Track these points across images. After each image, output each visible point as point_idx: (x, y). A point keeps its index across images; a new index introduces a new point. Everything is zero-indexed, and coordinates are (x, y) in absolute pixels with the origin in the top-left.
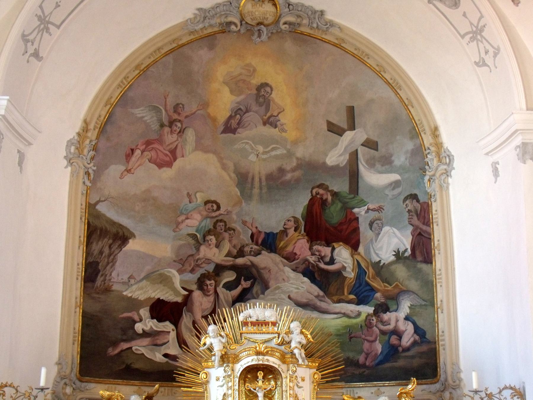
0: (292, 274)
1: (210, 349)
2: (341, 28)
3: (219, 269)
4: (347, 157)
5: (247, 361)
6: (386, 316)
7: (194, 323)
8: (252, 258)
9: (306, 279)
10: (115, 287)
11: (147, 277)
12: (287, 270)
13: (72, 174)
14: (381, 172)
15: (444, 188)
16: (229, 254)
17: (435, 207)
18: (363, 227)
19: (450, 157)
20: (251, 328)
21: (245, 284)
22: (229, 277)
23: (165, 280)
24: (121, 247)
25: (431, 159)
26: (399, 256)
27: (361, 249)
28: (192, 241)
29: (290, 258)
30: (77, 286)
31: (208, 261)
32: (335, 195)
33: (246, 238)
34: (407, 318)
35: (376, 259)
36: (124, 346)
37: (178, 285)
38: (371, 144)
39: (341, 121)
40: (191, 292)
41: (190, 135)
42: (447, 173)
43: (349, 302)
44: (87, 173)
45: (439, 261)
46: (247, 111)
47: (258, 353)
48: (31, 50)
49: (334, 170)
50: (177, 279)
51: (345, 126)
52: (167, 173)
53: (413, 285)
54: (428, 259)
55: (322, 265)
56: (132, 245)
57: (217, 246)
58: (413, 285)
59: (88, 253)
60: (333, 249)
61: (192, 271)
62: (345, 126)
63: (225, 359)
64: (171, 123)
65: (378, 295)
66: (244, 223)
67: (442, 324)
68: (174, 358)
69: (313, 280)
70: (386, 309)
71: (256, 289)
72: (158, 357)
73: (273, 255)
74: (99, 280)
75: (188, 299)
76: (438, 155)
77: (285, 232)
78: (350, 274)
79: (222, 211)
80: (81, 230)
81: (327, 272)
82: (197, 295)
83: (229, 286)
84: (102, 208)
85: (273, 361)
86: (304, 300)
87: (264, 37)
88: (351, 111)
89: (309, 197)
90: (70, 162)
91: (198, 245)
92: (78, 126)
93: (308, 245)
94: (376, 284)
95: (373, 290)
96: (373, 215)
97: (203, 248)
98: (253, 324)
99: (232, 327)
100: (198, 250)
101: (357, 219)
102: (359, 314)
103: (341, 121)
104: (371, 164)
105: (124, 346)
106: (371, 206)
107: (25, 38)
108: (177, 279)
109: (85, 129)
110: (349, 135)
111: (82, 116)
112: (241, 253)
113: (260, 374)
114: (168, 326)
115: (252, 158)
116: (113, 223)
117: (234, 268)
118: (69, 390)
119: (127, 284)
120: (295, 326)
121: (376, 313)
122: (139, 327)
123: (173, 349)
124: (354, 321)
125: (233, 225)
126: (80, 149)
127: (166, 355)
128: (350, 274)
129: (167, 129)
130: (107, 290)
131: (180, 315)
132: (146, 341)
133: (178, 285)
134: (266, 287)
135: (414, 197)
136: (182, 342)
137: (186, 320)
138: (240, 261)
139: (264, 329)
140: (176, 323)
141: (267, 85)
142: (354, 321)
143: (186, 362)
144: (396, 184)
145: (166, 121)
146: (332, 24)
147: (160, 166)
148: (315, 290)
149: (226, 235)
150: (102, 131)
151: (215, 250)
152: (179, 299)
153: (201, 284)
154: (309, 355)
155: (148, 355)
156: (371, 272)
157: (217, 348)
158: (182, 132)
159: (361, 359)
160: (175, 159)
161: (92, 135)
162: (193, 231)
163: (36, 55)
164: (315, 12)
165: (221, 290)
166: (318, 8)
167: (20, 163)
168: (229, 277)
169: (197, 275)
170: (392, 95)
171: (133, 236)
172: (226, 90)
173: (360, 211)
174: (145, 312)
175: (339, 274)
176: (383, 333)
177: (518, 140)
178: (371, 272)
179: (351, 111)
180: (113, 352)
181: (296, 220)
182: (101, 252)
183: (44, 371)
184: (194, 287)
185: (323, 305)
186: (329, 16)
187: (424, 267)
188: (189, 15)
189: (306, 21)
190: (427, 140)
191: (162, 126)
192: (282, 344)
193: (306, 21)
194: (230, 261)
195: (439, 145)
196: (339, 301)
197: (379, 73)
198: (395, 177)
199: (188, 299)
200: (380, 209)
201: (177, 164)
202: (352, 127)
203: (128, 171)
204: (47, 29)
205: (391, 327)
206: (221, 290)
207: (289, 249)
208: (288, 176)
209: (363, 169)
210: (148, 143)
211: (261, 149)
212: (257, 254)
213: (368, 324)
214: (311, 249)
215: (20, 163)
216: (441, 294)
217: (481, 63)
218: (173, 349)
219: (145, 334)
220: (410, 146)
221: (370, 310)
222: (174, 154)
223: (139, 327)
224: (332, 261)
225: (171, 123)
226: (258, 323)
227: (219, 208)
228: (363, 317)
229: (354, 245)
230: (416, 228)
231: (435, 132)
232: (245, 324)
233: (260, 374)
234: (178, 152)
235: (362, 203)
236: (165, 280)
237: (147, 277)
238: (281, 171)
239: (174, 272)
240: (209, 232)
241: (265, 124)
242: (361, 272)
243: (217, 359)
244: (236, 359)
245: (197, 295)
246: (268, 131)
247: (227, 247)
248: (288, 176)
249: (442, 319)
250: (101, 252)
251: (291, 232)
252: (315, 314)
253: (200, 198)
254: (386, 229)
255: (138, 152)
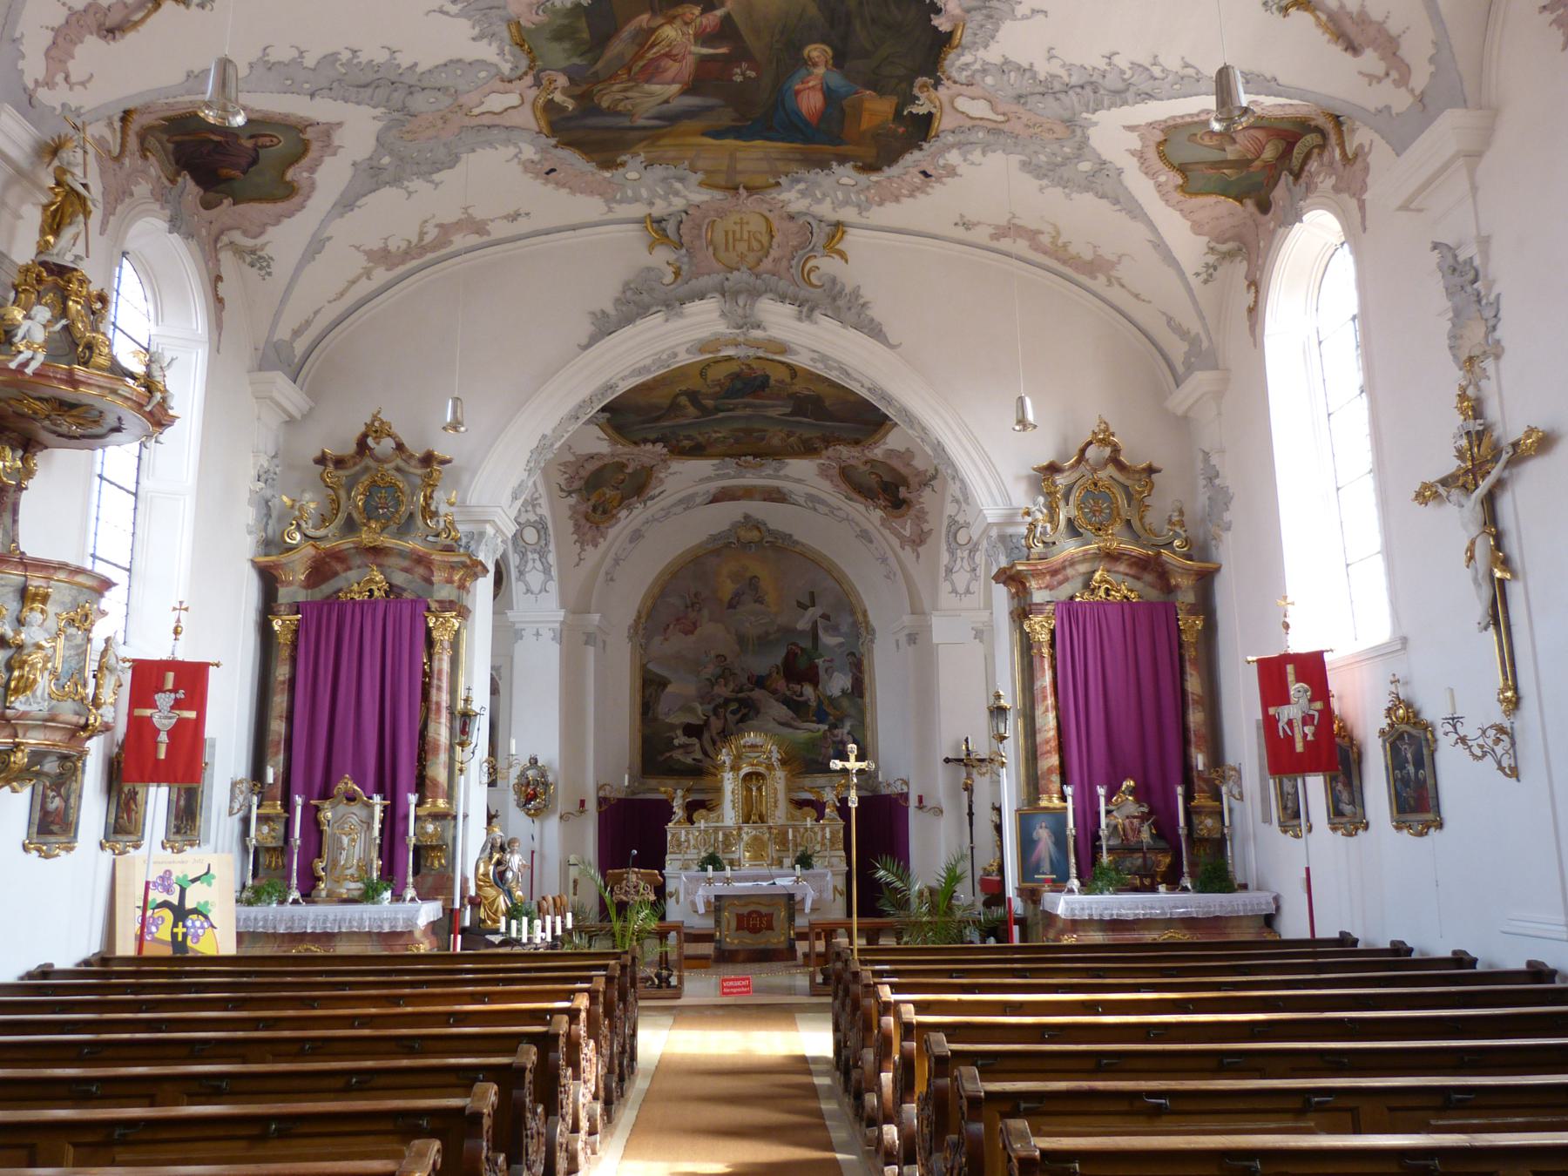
0: (776, 703)
1: (724, 762)
2: (803, 545)
3: (727, 701)
4: (810, 625)
5: (746, 769)
6: (836, 732)
7: (711, 738)
8: (749, 693)
9: (785, 707)
10: (660, 717)
11: (680, 709)
12: (773, 701)
13: (632, 648)
14: (833, 636)
15: (870, 651)
16: (733, 691)
17: (865, 662)
18: (821, 672)
19: (873, 630)
20: (748, 749)
21: (744, 711)
22: (734, 706)
23: (692, 710)
24: (663, 690)
25: (863, 631)
26: (843, 692)
27: (820, 687)
28: (707, 683)
29: (774, 692)
30: (638, 717)
31: (720, 696)
32: (802, 649)
33: (744, 680)
34: (849, 733)
35: (829, 694)
36: (668, 754)
37: (700, 712)
38: (825, 617)
39: (806, 600)
40: (708, 717)
41: (705, 612)
42: (872, 641)
43: (813, 722)
44: (641, 645)
45: (867, 699)
46: (743, 594)
47: (752, 765)
48: (609, 577)
49: (802, 633)
50: (699, 709)
51: (808, 604)
52: (691, 638)
53: (853, 712)
54: (861, 696)
55: (795, 697)
56: (670, 689)
57: (725, 686)
58: (853, 712)
59: (643, 697)
60: (802, 686)
61: (709, 703)
62: (808, 604)
63: (732, 769)
64: (693, 605)
65: (831, 718)
66: (743, 669)
67: (869, 738)
68: (700, 761)
69: (789, 707)
70: (836, 727)
71: (751, 714)
72: (689, 760)
73: (763, 691)
74: (651, 712)
75: (707, 723)
76: (867, 628)
77: (770, 675)
78: (813, 703)
79: (729, 660)
80: (638, 683)
81: (799, 702)
82: (713, 719)
83: (733, 713)
84: (650, 666)
85: (761, 769)
86: (783, 721)
87: (753, 550)
88: (812, 595)
89: (785, 651)
90: (630, 638)
91: (713, 685)
92: (634, 615)
93: (785, 684)
94: (830, 710)
95: (827, 714)
96: (827, 664)
97: (716, 688)
98: (749, 747)
99: (737, 748)
100: (712, 688)
101: (817, 667)
102: (819, 730)
103: (806, 600)
104: (826, 630)
105: (668, 754)
106: (827, 658)
107: (607, 573)
108: (699, 709)
109: (639, 617)
110: (811, 610)
111: (636, 606)
112: (741, 690)
113: (754, 777)
114: (694, 740)
115: (748, 625)
116: (658, 675)
117: (736, 700)
118: (636, 784)
119: (667, 714)
120: (774, 748)
121: (830, 729)
122: (676, 742)
123: (699, 755)
124: (817, 734)
125: (736, 671)
126: (636, 632)
127: (694, 759)
128: (813, 703)
129: (690, 609)
130: (655, 719)
131: (702, 733)
132: (681, 751)
133: (700, 712)
134: (758, 712)
135: (853, 654)
136: (705, 753)
137: (706, 736)
138: (741, 695)
139: (756, 749)
140: (700, 739)
141: (755, 577)
142: (817, 734)
143: (707, 763)
144: (841, 645)
145: (689, 603)
146: (797, 542)
147: (686, 633)
148: (791, 714)
149: (731, 678)
150: (649, 616)
151: (724, 689)
152: (701, 723)
153: (715, 712)
154: (783, 762)
155: (682, 758)
156: (826, 702)
157: (728, 763)
158: (700, 610)
159: (820, 759)
160: (696, 628)
161: (643, 620)
162: (708, 676)
163: (612, 580)
164: (786, 535)
165: (729, 716)
166: (788, 532)
167: (604, 647)
168: (734, 706)
169: (711, 706)
170: (838, 587)
171: (670, 682)
172: (729, 581)
173: (819, 662)
174: (679, 732)
175: (806, 703)
176: (834, 742)
177: (906, 631)
178: (826, 702)
179: (812, 595)
180: (661, 758)
181: (777, 666)
182: (651, 696)
183: (627, 777)
184: (711, 714)
185: (795, 724)
186: (796, 537)
187: (859, 700)
188: (704, 537)
189: (780, 541)
190: (861, 618)
191: (687, 607)
192: (767, 758)
193: (780, 541)
194: (733, 695)
195: (867, 623)
196: (807, 721)
197: (829, 572)
198: (841, 640)
199: (707, 723)
200: (831, 661)
201: (697, 632)
202: (813, 605)
203: (666, 639)
204: (618, 564)
205: (839, 739)
206: (729, 716)
207: (774, 685)
208: (772, 637)
209: (821, 633)
210: (678, 620)
211: (753, 619)
212: (752, 690)
213: (824, 736)
214: (787, 686)
215: (604, 647)
216: (868, 719)
217: (888, 577)
218: (699, 755)
219: (681, 746)
220: (850, 620)
221: (826, 727)
222: (695, 625)
223: (676, 742)
224: (801, 695)
225: (693, 605)
226: (753, 746)
227: (725, 659)
228: (821, 733)
229: (815, 683)
230: (854, 674)
231: (865, 613)
232: (744, 747)
233: (754, 777)
234: (698, 624)
235: (820, 656)
236: (692, 710)
237: (680, 709)
238: (767, 633)
239: (698, 705)
240: (720, 677)
241: (755, 602)
242: (820, 703)
243: (728, 769)
244: (739, 769)
245: (713, 719)
246: (757, 606)
247: (731, 686)
248: (772, 637)
249: (869, 734)
250: (651, 696)
251: (774, 675)
252: (791, 730)
253: (713, 654)
254: (836, 674)
255: (671, 626)
